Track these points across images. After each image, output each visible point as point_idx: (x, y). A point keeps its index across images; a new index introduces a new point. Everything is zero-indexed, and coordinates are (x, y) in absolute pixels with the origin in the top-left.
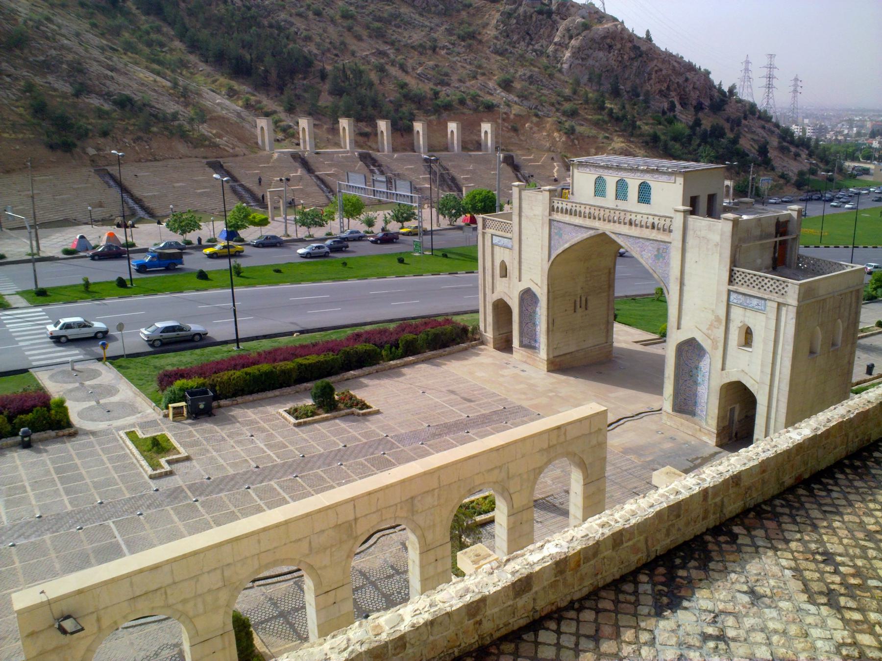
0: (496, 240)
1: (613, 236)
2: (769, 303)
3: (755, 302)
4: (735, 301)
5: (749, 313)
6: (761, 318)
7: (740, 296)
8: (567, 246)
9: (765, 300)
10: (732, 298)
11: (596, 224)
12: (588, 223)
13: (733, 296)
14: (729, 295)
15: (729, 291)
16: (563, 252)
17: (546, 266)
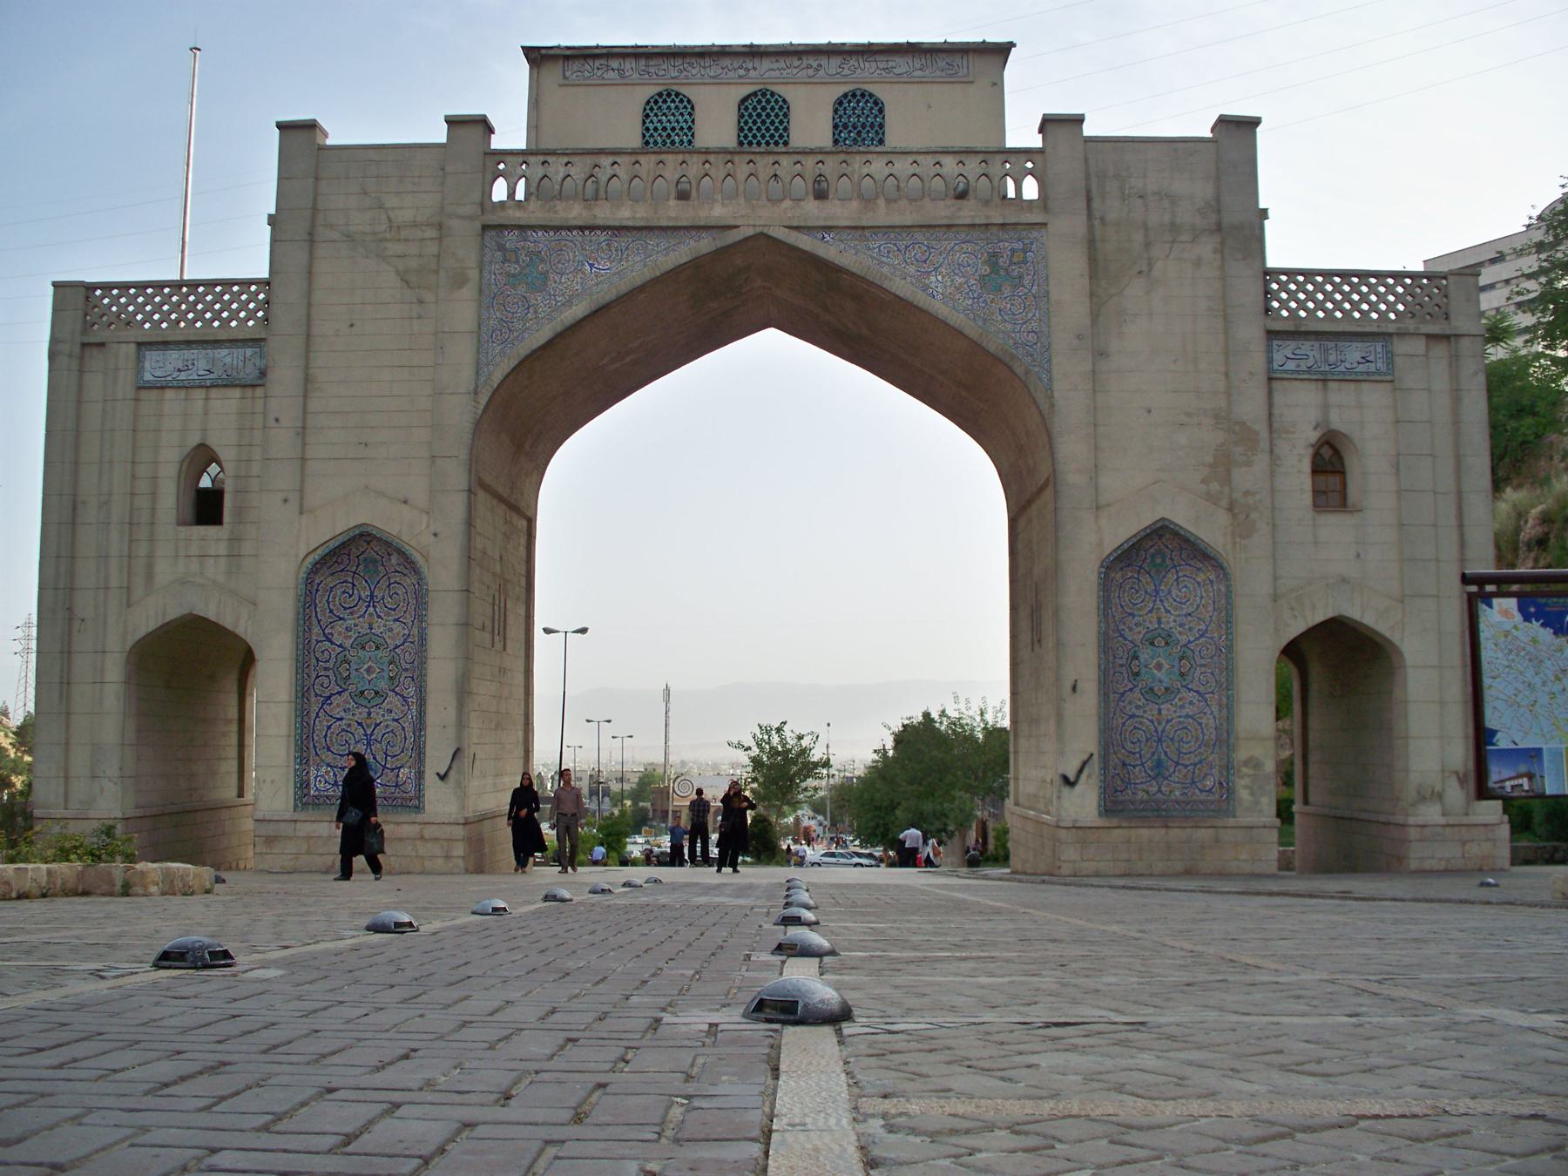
0: (158, 365)
1: (804, 242)
2: (1401, 347)
3: (1353, 353)
4: (1291, 366)
5: (1340, 395)
6: (1375, 397)
7: (1307, 347)
8: (579, 310)
9: (1385, 336)
10: (1278, 358)
11: (718, 212)
12: (674, 212)
13: (1283, 352)
14: (1269, 350)
15: (1271, 334)
16: (549, 344)
17: (460, 413)
